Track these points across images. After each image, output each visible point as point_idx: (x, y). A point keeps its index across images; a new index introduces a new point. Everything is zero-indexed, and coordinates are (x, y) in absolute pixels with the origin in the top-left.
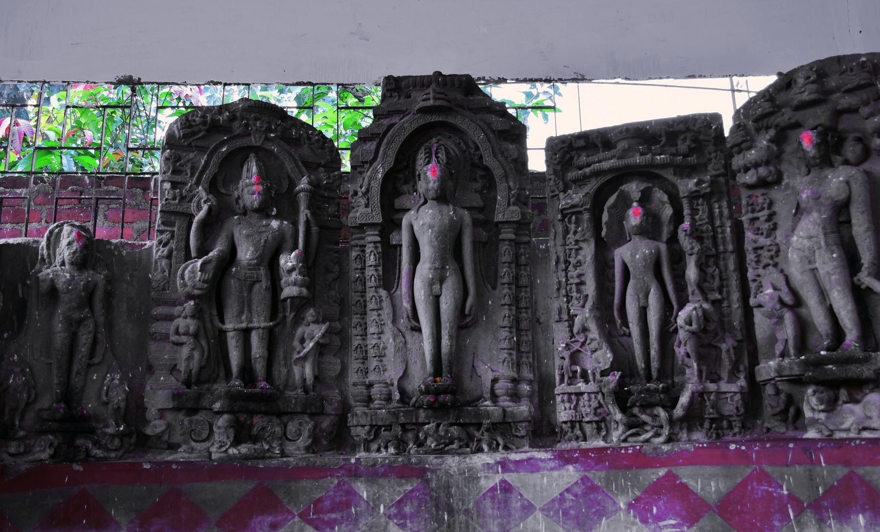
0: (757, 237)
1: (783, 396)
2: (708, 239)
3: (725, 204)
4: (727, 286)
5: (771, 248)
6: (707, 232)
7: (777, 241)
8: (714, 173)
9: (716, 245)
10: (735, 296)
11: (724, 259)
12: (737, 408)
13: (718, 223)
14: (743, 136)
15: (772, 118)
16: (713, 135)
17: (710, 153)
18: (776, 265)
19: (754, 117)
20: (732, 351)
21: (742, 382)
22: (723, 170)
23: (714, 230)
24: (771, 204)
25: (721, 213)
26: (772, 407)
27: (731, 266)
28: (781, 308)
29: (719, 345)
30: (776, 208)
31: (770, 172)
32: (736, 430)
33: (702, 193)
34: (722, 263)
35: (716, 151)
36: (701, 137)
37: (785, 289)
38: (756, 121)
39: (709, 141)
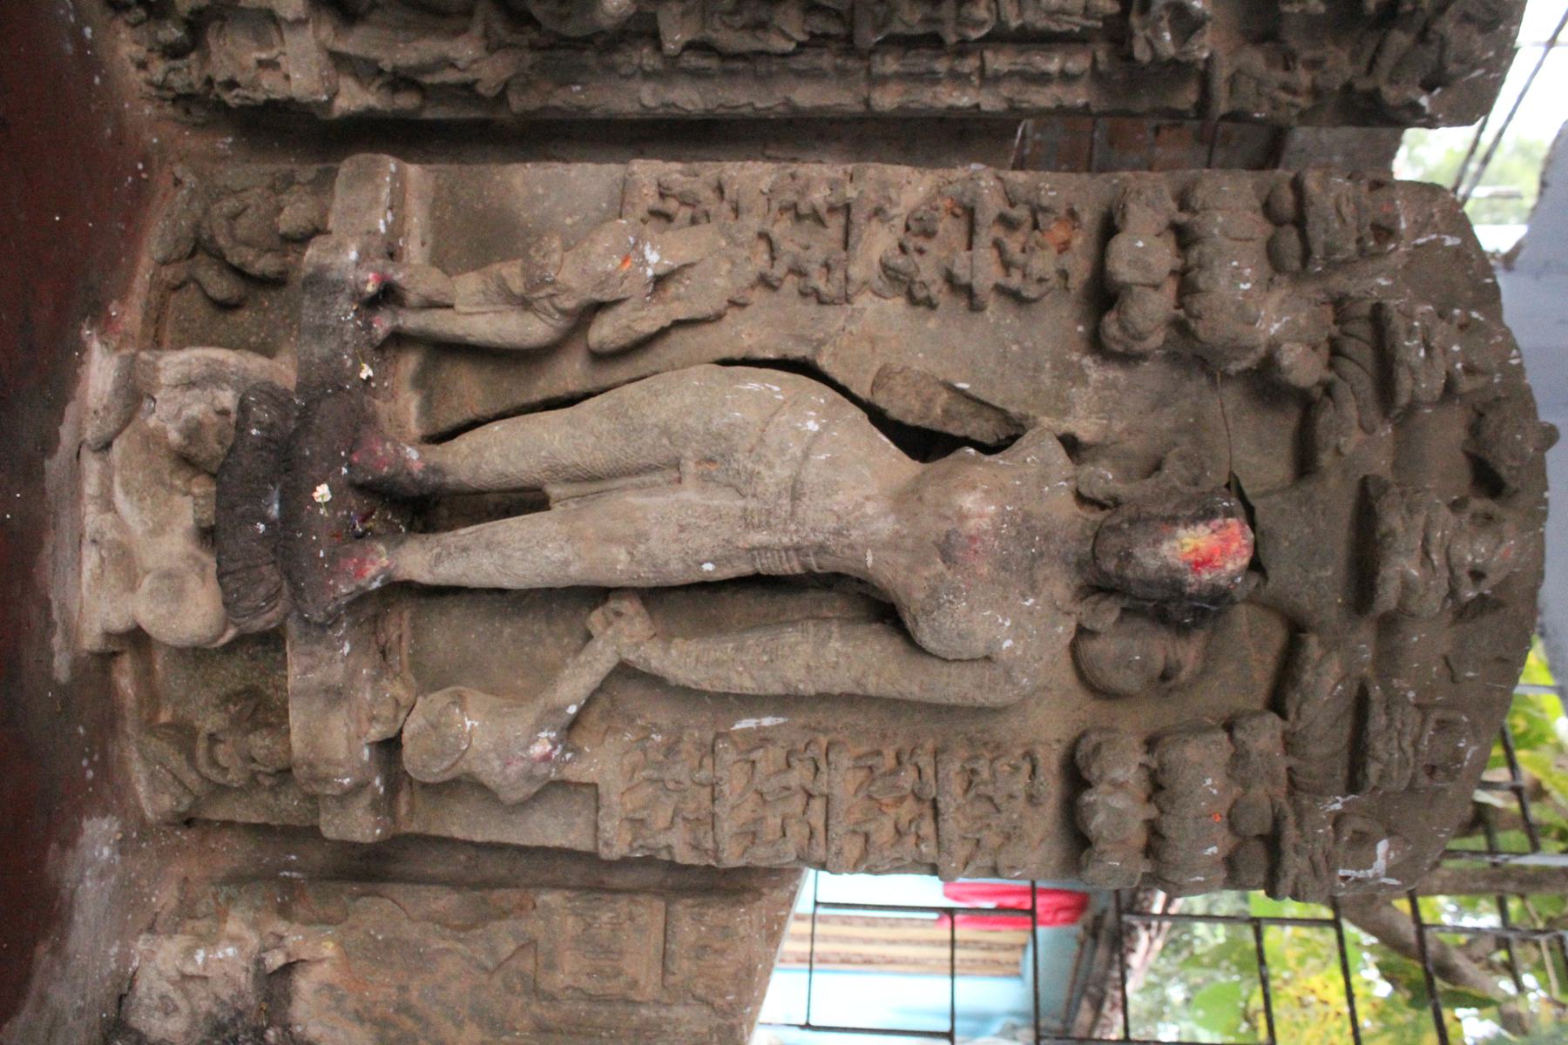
0: (899, 223)
1: (266, 264)
2: (928, 20)
3: (1078, 96)
4: (733, 74)
5: (838, 274)
6: (961, 22)
7: (865, 301)
8: (1222, 74)
9: (907, 43)
10: (689, 98)
11: (842, 73)
12: (231, 84)
13: (999, 61)
14: (1330, 250)
15: (1366, 387)
16: (1391, 94)
17: (1314, 64)
18: (766, 283)
19: (1398, 323)
20: (451, 76)
21: (353, 98)
22: (1222, 106)
23: (963, 49)
24: (1015, 297)
25: (1043, 79)
26: (234, 217)
27: (806, 96)
28: (563, 312)
29: (477, 30)
30: (994, 308)
31: (1140, 337)
32: (158, 69)
33: (1135, 20)
34: (826, 61)
35: (1316, 92)
36: (1400, 39)
37: (649, 320)
38: (1377, 316)
39: (1370, 70)
